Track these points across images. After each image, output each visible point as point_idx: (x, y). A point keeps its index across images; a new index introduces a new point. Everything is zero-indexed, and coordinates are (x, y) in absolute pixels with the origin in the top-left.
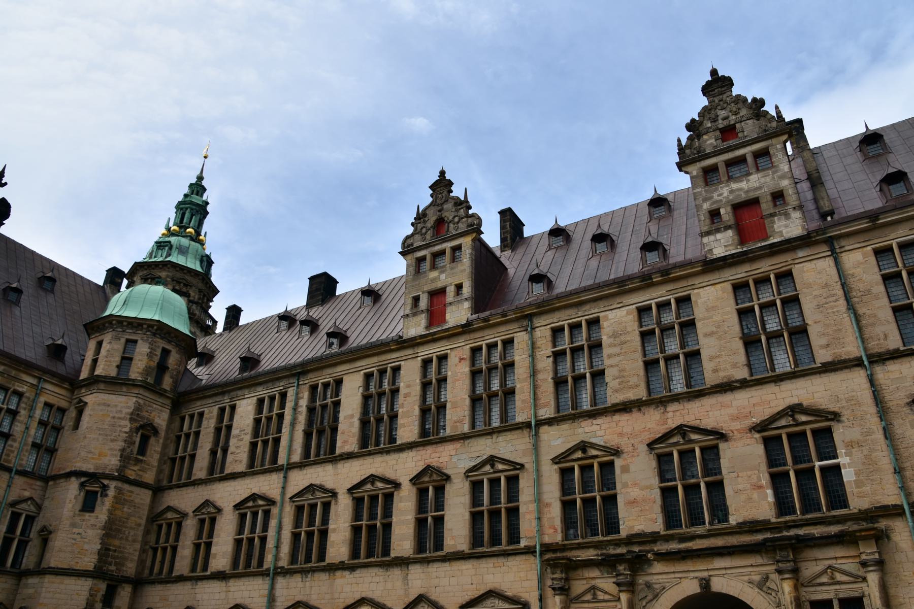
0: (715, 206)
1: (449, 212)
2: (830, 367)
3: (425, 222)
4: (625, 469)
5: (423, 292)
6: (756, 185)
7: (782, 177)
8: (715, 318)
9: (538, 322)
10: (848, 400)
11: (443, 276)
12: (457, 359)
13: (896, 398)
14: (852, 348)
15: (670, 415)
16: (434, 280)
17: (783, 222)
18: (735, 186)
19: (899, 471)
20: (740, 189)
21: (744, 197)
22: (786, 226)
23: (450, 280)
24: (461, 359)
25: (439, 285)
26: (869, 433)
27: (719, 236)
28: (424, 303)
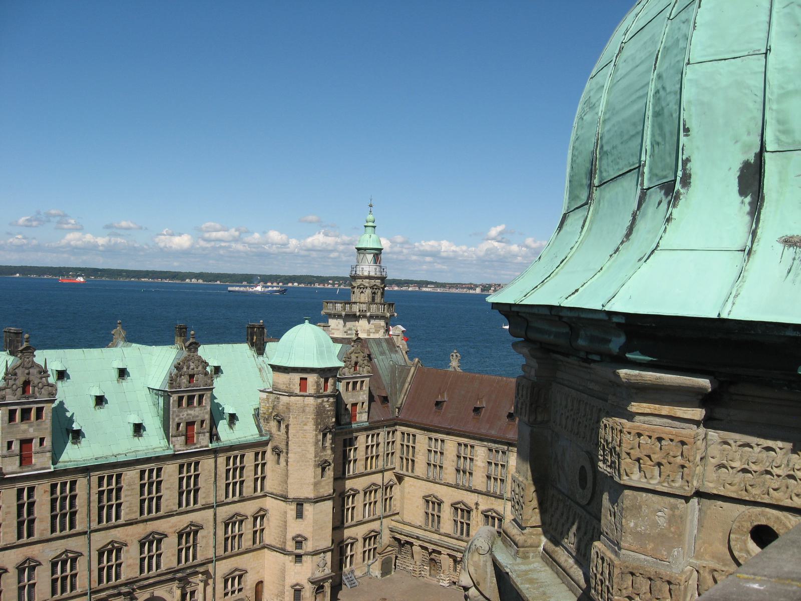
0: (180, 421)
1: (35, 379)
2: (206, 507)
3: (15, 380)
4: (127, 551)
5: (17, 439)
6: (197, 414)
7: (207, 413)
8: (171, 481)
9: (92, 474)
10: (206, 520)
11: (31, 430)
12: (43, 491)
13: (219, 520)
14: (212, 500)
15: (148, 526)
16: (25, 431)
17: (202, 437)
18: (189, 412)
19: (215, 547)
20: (191, 414)
21: (191, 420)
22: (203, 439)
23: (36, 434)
24: (45, 492)
25: (29, 436)
26: (209, 532)
27: (179, 438)
28: (16, 447)
